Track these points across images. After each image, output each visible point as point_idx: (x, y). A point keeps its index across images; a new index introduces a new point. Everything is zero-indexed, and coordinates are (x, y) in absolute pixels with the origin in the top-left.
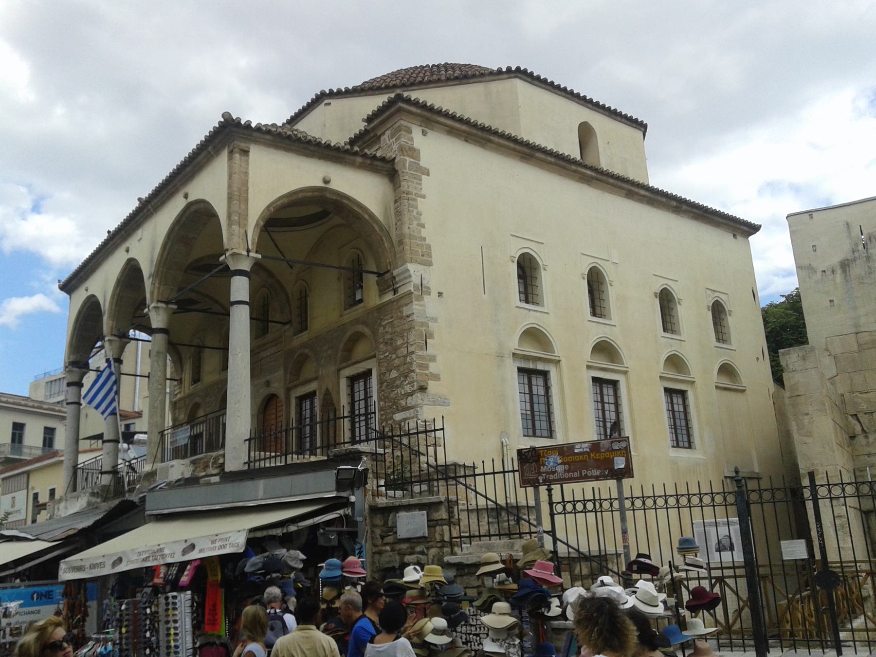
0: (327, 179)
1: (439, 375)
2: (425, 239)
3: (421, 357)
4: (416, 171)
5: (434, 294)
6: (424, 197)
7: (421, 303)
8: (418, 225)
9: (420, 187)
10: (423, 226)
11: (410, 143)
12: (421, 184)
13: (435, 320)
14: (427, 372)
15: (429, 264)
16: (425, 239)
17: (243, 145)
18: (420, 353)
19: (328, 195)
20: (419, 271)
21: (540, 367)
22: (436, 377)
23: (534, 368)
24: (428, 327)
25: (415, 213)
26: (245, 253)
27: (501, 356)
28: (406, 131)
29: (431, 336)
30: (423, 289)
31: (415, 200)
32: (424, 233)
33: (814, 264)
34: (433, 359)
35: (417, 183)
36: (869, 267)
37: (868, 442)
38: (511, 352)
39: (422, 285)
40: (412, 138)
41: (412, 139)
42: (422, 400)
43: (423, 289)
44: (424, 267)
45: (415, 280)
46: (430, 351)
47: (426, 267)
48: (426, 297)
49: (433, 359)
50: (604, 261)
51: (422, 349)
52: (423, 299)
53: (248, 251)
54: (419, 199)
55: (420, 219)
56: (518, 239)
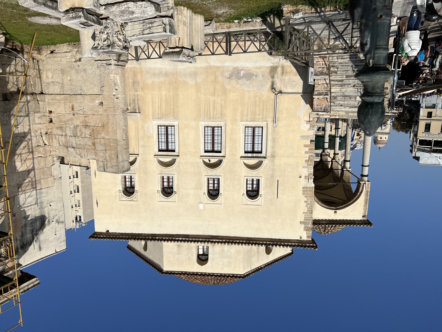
0: (336, 213)
1: (304, 147)
2: (305, 197)
4: (307, 222)
5: (303, 177)
7: (309, 173)
8: (308, 202)
9: (305, 216)
10: (305, 202)
11: (308, 232)
12: (305, 217)
13: (303, 167)
14: (310, 147)
16: (305, 197)
17: (364, 219)
18: (312, 154)
20: (310, 184)
21: (250, 155)
22: (305, 146)
23: (253, 154)
24: (307, 164)
25: (309, 206)
26: (366, 182)
28: (310, 236)
29: (306, 161)
30: (307, 178)
31: (308, 211)
32: (305, 199)
33: (57, 224)
34: (306, 153)
35: (307, 217)
36: (32, 226)
37: (40, 130)
38: (268, 159)
39: (309, 179)
40: (307, 234)
42: (313, 137)
44: (306, 186)
45: (311, 181)
46: (307, 155)
47: (305, 186)
48: (307, 175)
49: (306, 153)
50: (211, 203)
51: (311, 156)
52: (308, 174)
53: (365, 183)
54: (307, 212)
55: (306, 204)
56: (257, 205)
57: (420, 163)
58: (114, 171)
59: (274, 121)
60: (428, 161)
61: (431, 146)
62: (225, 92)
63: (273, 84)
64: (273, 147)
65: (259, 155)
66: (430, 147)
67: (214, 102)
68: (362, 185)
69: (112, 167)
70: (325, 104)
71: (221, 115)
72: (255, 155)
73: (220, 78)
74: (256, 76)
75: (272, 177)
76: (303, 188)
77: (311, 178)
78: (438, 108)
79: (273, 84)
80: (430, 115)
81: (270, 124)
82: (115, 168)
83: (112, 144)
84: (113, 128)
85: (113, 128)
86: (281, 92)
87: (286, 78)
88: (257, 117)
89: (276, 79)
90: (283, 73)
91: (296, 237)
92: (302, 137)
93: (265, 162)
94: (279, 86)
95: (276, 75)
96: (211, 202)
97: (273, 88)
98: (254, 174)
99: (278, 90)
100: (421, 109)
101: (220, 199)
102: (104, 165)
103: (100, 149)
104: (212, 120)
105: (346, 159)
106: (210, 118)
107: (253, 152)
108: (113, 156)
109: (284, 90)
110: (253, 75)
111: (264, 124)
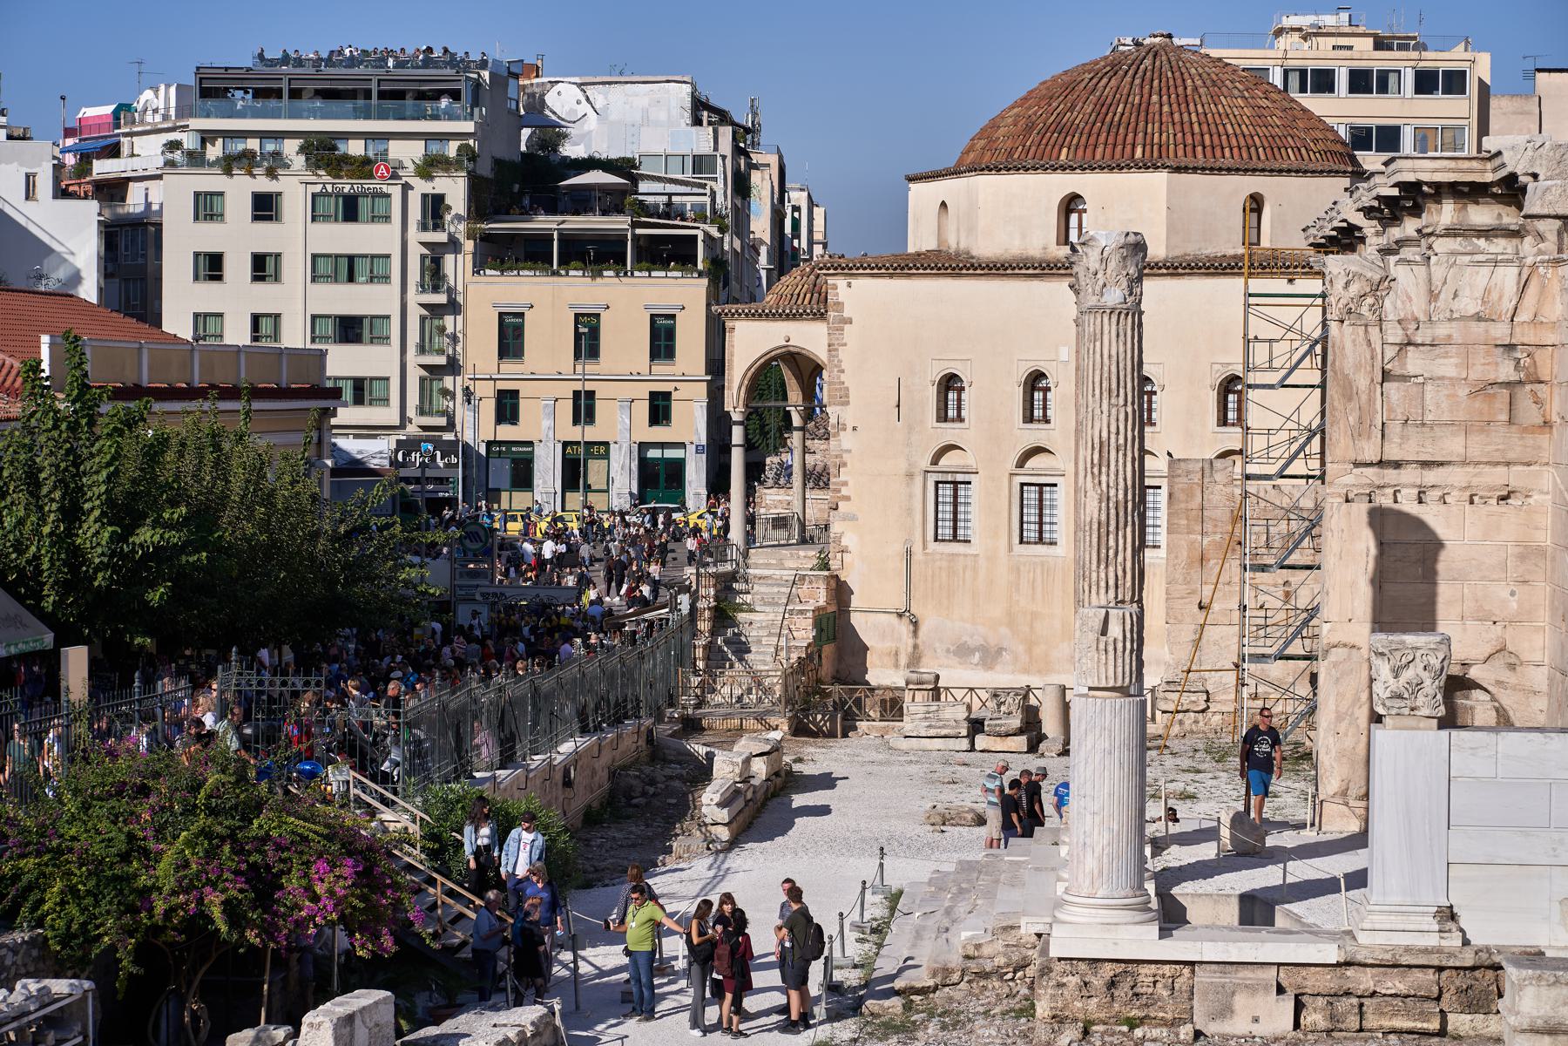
3: (835, 483)
5: (849, 428)
6: (845, 345)
10: (843, 371)
13: (849, 451)
15: (847, 403)
19: (791, 349)
21: (960, 478)
22: (848, 498)
27: (910, 475)
29: (845, 465)
30: (841, 426)
31: (837, 350)
32: (843, 377)
34: (845, 484)
41: (837, 294)
43: (841, 426)
46: (843, 478)
48: (842, 433)
49: (845, 484)
57: (687, 88)
58: (1182, 464)
59: (909, 553)
60: (645, 102)
61: (636, 238)
62: (1011, 619)
63: (915, 632)
64: (911, 496)
65: (940, 477)
66: (639, 231)
67: (1033, 599)
68: (741, 403)
69: (1188, 473)
70: (803, 590)
71: (1018, 569)
72: (950, 477)
73: (1021, 648)
74: (948, 651)
75: (910, 429)
76: (847, 403)
77: (833, 427)
78: (625, 447)
79: (915, 632)
80: (660, 409)
81: (917, 549)
82: (1180, 472)
83: (1184, 522)
84: (1176, 557)
85: (1176, 557)
86: (900, 615)
87: (889, 645)
88: (944, 564)
89: (911, 642)
90: (896, 654)
91: (858, 283)
92: (853, 518)
93: (925, 463)
94: (904, 628)
95: (910, 649)
96: (1042, 364)
97: (915, 624)
98: (950, 433)
99: (905, 620)
100: (704, 442)
101: (1022, 373)
102: (1211, 475)
103: (1219, 512)
104: (1037, 560)
105: (801, 433)
106: (1042, 564)
107: (955, 483)
108: (1182, 497)
109: (894, 619)
110: (956, 653)
111: (933, 546)
